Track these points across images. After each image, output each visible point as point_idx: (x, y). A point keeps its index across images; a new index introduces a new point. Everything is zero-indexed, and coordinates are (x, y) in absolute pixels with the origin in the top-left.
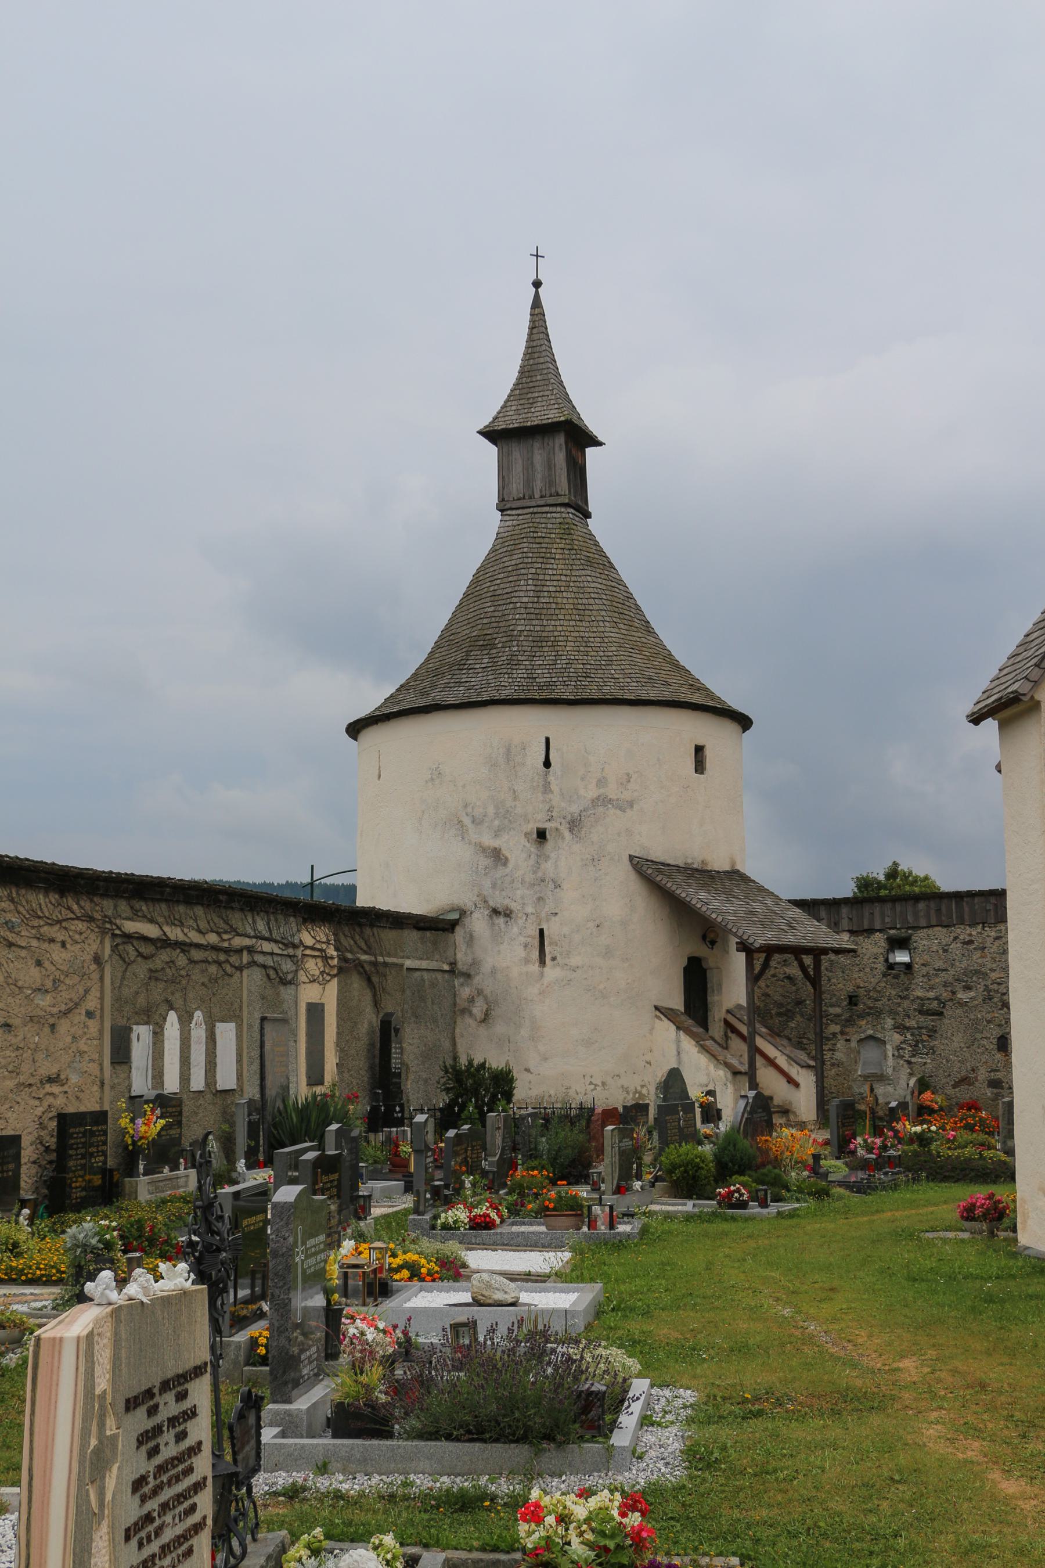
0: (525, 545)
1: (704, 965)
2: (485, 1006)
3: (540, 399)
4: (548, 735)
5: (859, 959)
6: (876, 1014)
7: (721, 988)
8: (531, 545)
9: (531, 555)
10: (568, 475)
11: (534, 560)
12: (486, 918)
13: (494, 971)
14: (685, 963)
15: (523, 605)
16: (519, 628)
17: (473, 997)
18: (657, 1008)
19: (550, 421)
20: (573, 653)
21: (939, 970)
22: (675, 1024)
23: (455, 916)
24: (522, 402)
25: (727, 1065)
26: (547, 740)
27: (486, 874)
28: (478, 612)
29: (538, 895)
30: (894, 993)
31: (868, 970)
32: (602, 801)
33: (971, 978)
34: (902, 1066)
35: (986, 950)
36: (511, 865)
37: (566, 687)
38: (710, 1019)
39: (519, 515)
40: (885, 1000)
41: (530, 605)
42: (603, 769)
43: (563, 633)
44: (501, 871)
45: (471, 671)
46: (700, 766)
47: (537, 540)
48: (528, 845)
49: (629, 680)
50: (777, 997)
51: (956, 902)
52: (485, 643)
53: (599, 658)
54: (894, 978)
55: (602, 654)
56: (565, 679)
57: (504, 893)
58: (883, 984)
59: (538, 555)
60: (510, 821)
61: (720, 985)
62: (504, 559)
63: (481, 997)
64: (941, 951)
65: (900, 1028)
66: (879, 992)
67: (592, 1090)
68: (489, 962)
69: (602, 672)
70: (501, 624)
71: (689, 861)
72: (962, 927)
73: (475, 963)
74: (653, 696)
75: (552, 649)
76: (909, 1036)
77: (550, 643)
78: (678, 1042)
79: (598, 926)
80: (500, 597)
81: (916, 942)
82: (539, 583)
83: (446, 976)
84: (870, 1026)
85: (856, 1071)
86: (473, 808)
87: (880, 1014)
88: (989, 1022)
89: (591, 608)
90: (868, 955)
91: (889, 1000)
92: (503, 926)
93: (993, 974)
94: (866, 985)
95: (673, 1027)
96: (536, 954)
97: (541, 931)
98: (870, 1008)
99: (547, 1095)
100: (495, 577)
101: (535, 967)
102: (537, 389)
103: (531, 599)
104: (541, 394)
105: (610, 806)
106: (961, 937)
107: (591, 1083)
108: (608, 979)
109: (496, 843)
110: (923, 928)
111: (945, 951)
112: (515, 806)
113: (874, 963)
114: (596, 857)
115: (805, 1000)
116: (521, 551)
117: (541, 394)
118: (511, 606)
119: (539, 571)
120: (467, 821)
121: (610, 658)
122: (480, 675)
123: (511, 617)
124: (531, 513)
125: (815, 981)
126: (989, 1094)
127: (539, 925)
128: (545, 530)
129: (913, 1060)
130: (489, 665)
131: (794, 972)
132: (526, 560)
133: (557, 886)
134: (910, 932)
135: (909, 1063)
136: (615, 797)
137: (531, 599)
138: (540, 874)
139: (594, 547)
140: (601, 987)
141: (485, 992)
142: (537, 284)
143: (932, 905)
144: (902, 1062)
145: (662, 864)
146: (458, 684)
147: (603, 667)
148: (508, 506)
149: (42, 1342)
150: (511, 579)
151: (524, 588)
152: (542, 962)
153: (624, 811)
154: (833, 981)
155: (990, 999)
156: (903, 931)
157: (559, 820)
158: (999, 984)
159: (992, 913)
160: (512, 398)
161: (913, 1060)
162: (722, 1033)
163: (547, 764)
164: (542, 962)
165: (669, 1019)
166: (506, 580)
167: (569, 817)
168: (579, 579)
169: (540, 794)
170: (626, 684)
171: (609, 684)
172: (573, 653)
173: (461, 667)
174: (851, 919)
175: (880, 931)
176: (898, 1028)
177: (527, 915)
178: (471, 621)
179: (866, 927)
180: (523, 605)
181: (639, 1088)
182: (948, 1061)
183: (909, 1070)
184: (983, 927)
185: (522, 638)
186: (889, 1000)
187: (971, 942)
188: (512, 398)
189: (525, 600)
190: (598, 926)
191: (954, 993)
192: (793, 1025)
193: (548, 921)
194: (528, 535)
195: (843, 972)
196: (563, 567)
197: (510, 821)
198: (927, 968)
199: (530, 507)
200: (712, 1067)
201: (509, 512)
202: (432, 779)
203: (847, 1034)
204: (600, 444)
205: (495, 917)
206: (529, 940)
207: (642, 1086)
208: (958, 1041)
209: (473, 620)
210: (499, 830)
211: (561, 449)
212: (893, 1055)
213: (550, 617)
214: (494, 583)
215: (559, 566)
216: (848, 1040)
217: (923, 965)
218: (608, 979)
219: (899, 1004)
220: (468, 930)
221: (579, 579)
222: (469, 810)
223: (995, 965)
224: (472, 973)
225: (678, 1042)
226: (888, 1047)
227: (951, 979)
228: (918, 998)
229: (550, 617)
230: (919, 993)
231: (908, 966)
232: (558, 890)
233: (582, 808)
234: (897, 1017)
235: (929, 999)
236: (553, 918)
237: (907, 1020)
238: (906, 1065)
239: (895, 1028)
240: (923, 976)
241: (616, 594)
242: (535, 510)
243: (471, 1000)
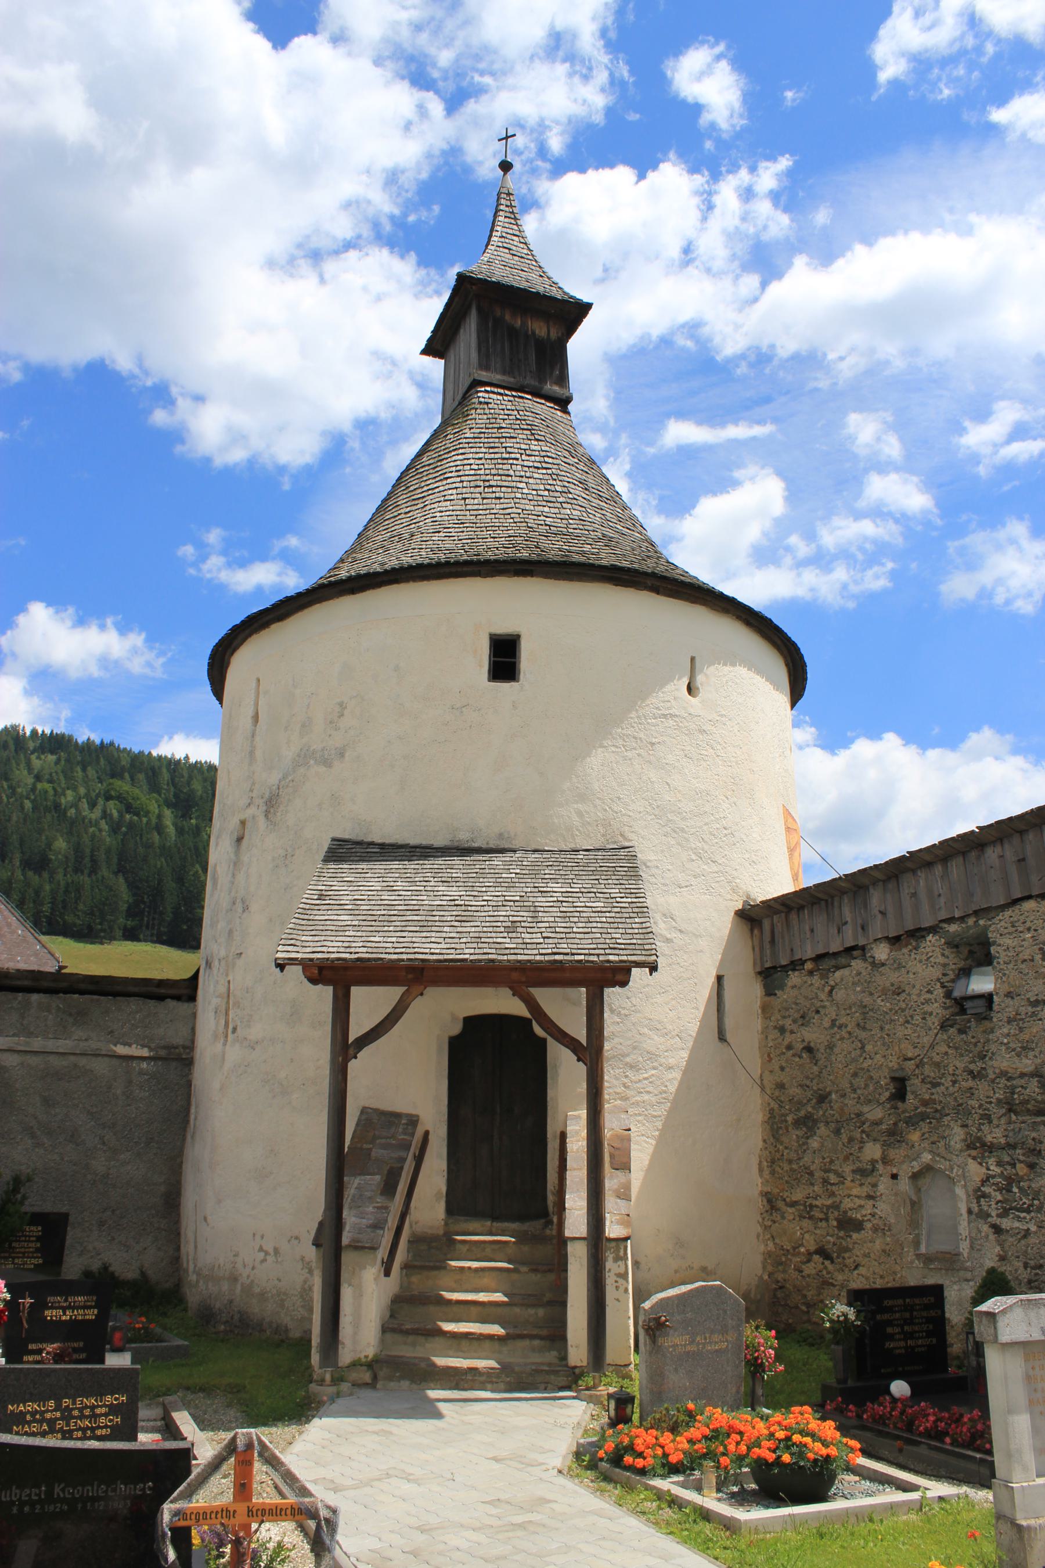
5: (903, 996)
30: (960, 1065)
32: (305, 757)
34: (987, 1237)
40: (947, 1081)
58: (943, 1048)
65: (978, 1147)
66: (937, 1065)
91: (954, 1082)
98: (925, 1103)
108: (292, 1060)
114: (290, 850)
115: (830, 1093)
133: (246, 908)
134: (981, 922)
135: (997, 1229)
154: (868, 1048)
156: (971, 921)
161: (1006, 1223)
174: (883, 913)
175: (933, 930)
179: (910, 926)
183: (998, 1249)
198: (1017, 1001)
212: (970, 1212)
228: (1003, 1074)
230: (1003, 1061)
235: (1022, 1075)
237: (986, 1128)
239: (969, 1147)
240: (1009, 1021)
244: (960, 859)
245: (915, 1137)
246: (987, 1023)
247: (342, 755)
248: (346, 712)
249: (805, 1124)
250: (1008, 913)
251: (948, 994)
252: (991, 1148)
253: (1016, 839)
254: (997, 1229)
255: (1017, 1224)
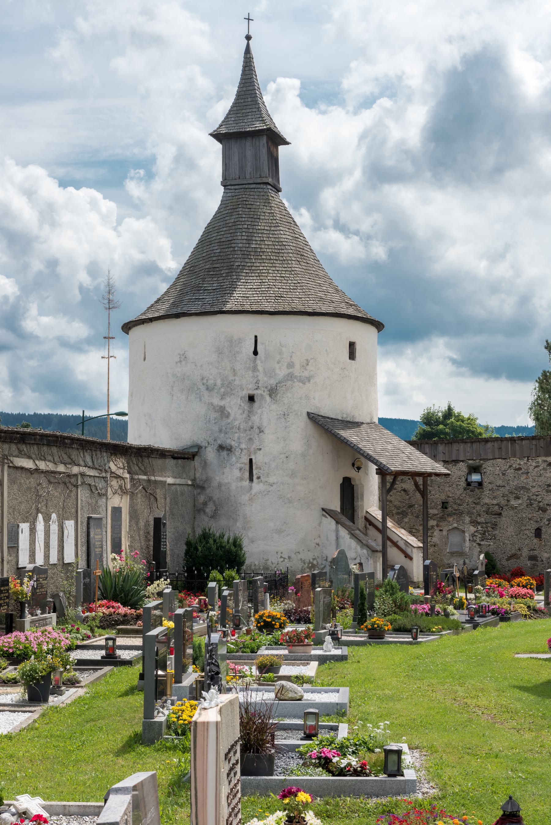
0: (240, 209)
1: (353, 483)
2: (214, 508)
3: (250, 114)
4: (256, 334)
6: (459, 514)
7: (363, 497)
8: (244, 210)
9: (244, 216)
10: (268, 164)
11: (246, 219)
12: (215, 451)
13: (220, 485)
14: (341, 481)
15: (239, 249)
16: (237, 264)
17: (206, 502)
18: (323, 510)
19: (257, 129)
20: (272, 281)
21: (499, 486)
22: (335, 520)
23: (196, 450)
24: (238, 115)
25: (368, 547)
26: (256, 337)
27: (215, 423)
28: (209, 252)
29: (249, 437)
30: (470, 500)
31: (454, 486)
32: (291, 377)
33: (520, 491)
35: (529, 474)
36: (231, 418)
37: (268, 303)
38: (355, 516)
39: (236, 189)
40: (465, 505)
41: (244, 249)
42: (291, 357)
43: (265, 268)
44: (225, 421)
45: (206, 292)
46: (352, 356)
47: (248, 206)
48: (242, 404)
49: (308, 299)
50: (397, 503)
51: (511, 443)
52: (215, 273)
53: (288, 285)
54: (471, 491)
55: (290, 282)
56: (267, 298)
57: (227, 436)
59: (248, 216)
60: (231, 389)
61: (362, 495)
62: (226, 219)
63: (211, 501)
64: (501, 474)
65: (475, 523)
66: (461, 500)
67: (282, 562)
68: (218, 479)
69: (291, 293)
70: (225, 261)
71: (345, 416)
72: (515, 459)
73: (208, 480)
74: (324, 309)
75: (258, 278)
76: (480, 528)
77: (257, 275)
78: (337, 531)
79: (287, 457)
80: (225, 243)
81: (485, 468)
82: (250, 234)
83: (190, 488)
84: (455, 521)
85: (446, 549)
86: (207, 380)
87: (462, 514)
88: (530, 519)
89: (283, 251)
90: (455, 476)
91: (467, 505)
92: (226, 456)
93: (534, 489)
94: (453, 495)
95: (334, 522)
96: (247, 475)
97: (251, 460)
98: (456, 510)
99: (253, 564)
100: (221, 230)
101: (246, 483)
102: (248, 107)
103: (244, 245)
104: (250, 110)
105: (295, 380)
106: (514, 466)
107: (281, 557)
108: (293, 491)
109: (222, 403)
110: (490, 459)
111: (504, 474)
112: (235, 380)
113: (459, 481)
115: (414, 505)
116: (237, 213)
117: (250, 110)
118: (232, 249)
119: (249, 227)
120: (203, 388)
121: (296, 285)
122: (211, 294)
123: (231, 256)
124: (244, 188)
125: (424, 493)
126: (529, 565)
127: (249, 456)
128: (253, 200)
129: (482, 543)
130: (218, 288)
131: (408, 487)
132: (241, 219)
133: (261, 431)
134: (481, 462)
135: (479, 545)
136: (299, 375)
137: (244, 245)
138: (250, 424)
139: (285, 212)
140: (289, 496)
141: (214, 499)
142: (248, 38)
143: (496, 444)
144: (475, 544)
145: (328, 418)
146: (197, 300)
147: (292, 291)
148: (228, 183)
149: (198, 724)
150: (231, 231)
151: (240, 238)
152: (251, 479)
153: (304, 384)
154: (432, 492)
155: (531, 505)
156: (477, 461)
157: (262, 389)
158: (537, 495)
159: (534, 450)
160: (232, 112)
161: (482, 543)
162: (363, 526)
163: (255, 353)
164: (251, 479)
165: (331, 517)
166: (228, 232)
167: (269, 387)
168: (276, 233)
169: (250, 372)
170: (306, 302)
171: (295, 301)
172: (272, 281)
173: (199, 289)
174: (444, 454)
175: (463, 461)
176: (473, 522)
177: (242, 450)
178: (204, 258)
179: (454, 458)
180: (239, 249)
181: (311, 560)
182: (504, 544)
183: (479, 550)
184: (528, 459)
185: (239, 270)
186: (467, 505)
187: (520, 469)
188: (232, 112)
189: (240, 245)
190: (287, 457)
191: (508, 501)
192: (407, 520)
193: (255, 453)
194: (242, 203)
195: (439, 487)
196: (265, 224)
197: (231, 389)
199: (243, 184)
200: (359, 548)
201: (229, 187)
202: (180, 361)
203: (441, 526)
204: (287, 143)
205: (221, 451)
206: (243, 465)
207: (314, 559)
208: (510, 531)
209: (207, 257)
210: (224, 395)
211: (264, 146)
212: (470, 540)
213: (257, 257)
214: (220, 233)
215: (263, 224)
216: (440, 530)
217: (489, 483)
218: (293, 491)
219: (474, 508)
220: (203, 459)
221: (276, 233)
222: (205, 381)
223: (534, 484)
224: (206, 486)
225: (337, 531)
226: (467, 535)
227: (507, 493)
228: (486, 504)
229: (257, 257)
230: (487, 500)
231: (480, 484)
232: (261, 434)
233: (277, 381)
234: (473, 516)
235: (493, 505)
236: (258, 452)
237: (478, 518)
238: (477, 546)
239: (471, 523)
240: (489, 490)
241: (298, 243)
242: (247, 186)
243: (205, 504)
244: (478, 443)
245: (451, 519)
246: (481, 490)
247: (309, 381)
248: (309, 364)
249: (402, 514)
250: (491, 461)
251: (466, 480)
252: (479, 523)
253: (499, 442)
254: (479, 545)
255: (486, 543)
